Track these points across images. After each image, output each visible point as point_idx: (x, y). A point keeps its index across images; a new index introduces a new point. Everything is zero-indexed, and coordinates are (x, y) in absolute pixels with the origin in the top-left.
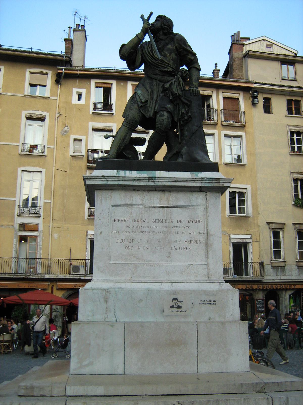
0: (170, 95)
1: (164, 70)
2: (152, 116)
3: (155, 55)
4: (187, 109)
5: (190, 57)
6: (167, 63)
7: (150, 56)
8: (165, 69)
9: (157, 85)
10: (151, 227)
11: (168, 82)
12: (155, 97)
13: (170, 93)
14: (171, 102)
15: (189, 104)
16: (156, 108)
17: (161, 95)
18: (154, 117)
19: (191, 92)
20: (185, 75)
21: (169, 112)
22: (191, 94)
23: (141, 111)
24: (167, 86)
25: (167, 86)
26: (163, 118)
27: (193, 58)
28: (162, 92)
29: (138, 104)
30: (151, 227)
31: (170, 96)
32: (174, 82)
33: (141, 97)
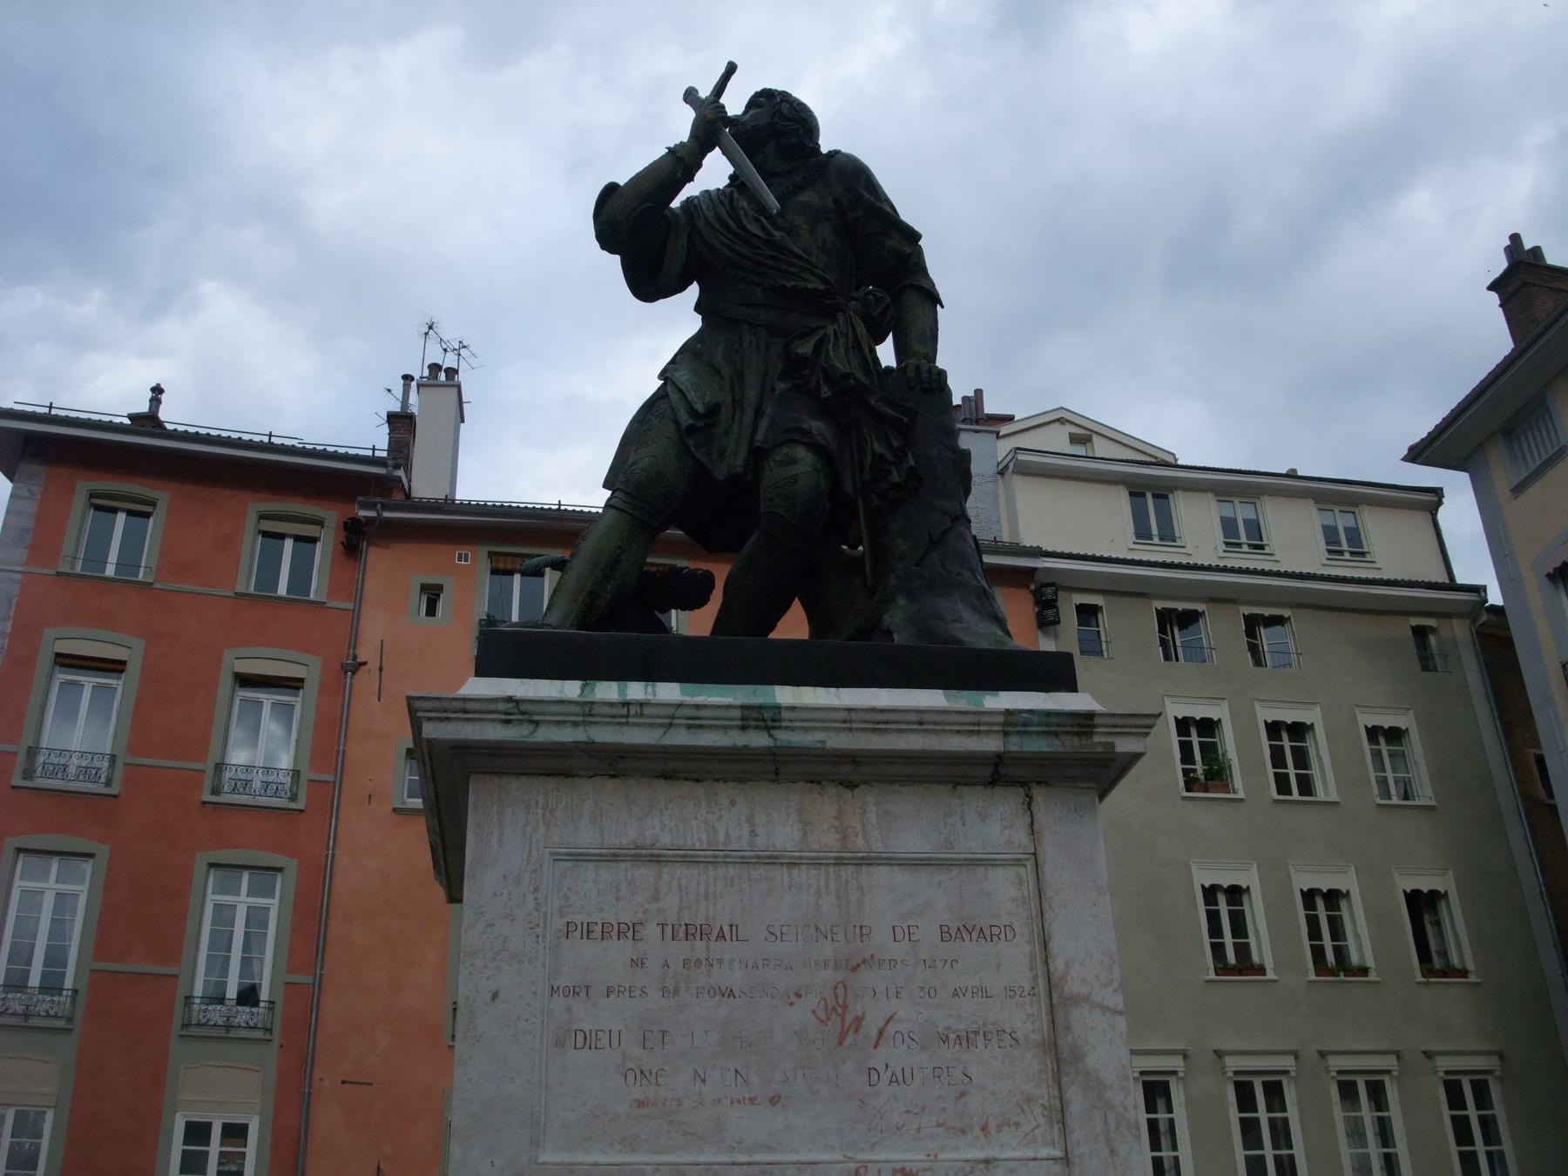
0: (821, 382)
1: (789, 285)
2: (739, 470)
3: (748, 227)
4: (895, 444)
5: (894, 242)
6: (799, 257)
7: (728, 235)
8: (793, 283)
9: (757, 346)
10: (760, 964)
11: (806, 334)
12: (752, 394)
13: (821, 376)
14: (825, 410)
15: (905, 419)
16: (760, 436)
17: (781, 386)
18: (749, 477)
19: (911, 374)
20: (879, 310)
21: (816, 448)
22: (912, 384)
23: (693, 449)
24: (805, 348)
25: (805, 348)
26: (794, 469)
27: (908, 250)
28: (782, 378)
29: (676, 422)
30: (760, 964)
31: (818, 386)
32: (832, 336)
33: (691, 396)
